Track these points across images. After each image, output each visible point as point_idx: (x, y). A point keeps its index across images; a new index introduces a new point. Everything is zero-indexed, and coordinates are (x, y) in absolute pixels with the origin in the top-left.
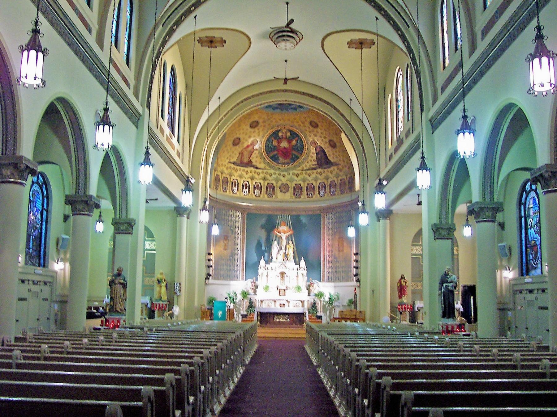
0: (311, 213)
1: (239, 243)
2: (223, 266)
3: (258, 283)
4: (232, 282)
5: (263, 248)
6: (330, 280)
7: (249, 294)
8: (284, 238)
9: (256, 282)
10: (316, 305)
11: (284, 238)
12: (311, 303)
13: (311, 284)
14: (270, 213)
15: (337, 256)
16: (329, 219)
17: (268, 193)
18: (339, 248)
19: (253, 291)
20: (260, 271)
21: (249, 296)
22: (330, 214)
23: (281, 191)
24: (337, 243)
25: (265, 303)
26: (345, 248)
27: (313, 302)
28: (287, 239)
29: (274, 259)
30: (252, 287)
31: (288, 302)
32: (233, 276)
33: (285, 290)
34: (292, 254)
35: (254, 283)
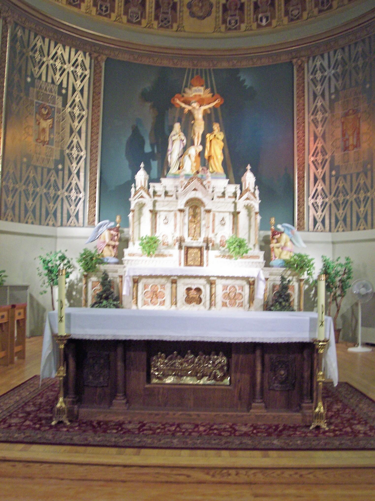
0: (265, 62)
1: (84, 129)
2: (36, 186)
3: (129, 232)
4: (61, 231)
5: (148, 149)
6: (319, 225)
7: (102, 262)
8: (199, 115)
9: (125, 230)
10: (289, 291)
11: (199, 115)
12: (274, 286)
13: (274, 234)
14: (166, 63)
15: (338, 162)
16: (314, 72)
17: (161, 16)
18: (345, 141)
19: (114, 252)
20: (134, 202)
21: (102, 267)
22: (318, 58)
23: (192, 14)
24: (338, 133)
25: (145, 287)
26: (364, 138)
27: (279, 283)
28: (207, 117)
29: (174, 170)
30: (113, 243)
31: (212, 284)
32: (65, 216)
33: (200, 249)
34: (220, 158)
35: (118, 230)
